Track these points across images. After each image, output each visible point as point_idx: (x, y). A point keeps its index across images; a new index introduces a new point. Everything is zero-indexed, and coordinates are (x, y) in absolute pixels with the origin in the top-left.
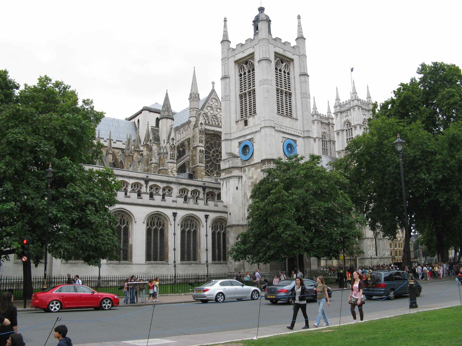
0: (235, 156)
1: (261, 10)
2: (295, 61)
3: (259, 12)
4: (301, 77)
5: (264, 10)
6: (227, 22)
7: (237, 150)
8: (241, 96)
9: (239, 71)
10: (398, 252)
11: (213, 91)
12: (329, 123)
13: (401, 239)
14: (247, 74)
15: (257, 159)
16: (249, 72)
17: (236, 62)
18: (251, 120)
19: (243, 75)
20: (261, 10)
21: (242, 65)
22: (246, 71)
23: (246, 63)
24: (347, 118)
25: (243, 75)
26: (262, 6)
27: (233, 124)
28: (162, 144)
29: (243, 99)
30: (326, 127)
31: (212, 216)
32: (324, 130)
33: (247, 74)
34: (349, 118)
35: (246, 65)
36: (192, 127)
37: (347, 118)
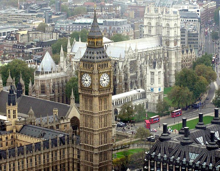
0: (150, 90)
7: (150, 89)
10: (188, 64)
11: (130, 47)
12: (159, 17)
13: (190, 57)
15: (154, 92)
17: (151, 72)
18: (153, 84)
24: (168, 23)
27: (149, 84)
28: (120, 69)
30: (158, 19)
31: (146, 101)
32: (157, 21)
34: (169, 23)
36: (126, 61)
37: (168, 23)
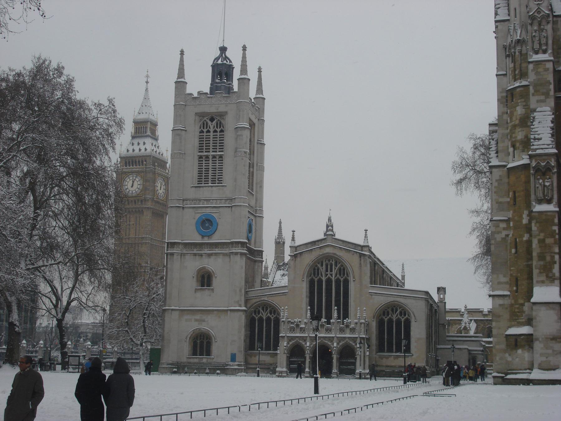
1: (223, 50)
2: (256, 125)
3: (219, 52)
4: (260, 145)
5: (226, 51)
6: (184, 56)
8: (201, 157)
9: (200, 128)
14: (212, 134)
16: (215, 131)
17: (196, 113)
19: (205, 133)
20: (223, 50)
21: (205, 121)
22: (212, 130)
23: (212, 120)
25: (205, 133)
26: (225, 46)
29: (204, 162)
33: (212, 134)
35: (212, 122)
